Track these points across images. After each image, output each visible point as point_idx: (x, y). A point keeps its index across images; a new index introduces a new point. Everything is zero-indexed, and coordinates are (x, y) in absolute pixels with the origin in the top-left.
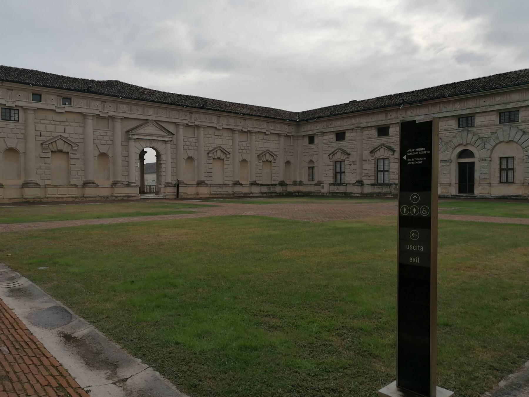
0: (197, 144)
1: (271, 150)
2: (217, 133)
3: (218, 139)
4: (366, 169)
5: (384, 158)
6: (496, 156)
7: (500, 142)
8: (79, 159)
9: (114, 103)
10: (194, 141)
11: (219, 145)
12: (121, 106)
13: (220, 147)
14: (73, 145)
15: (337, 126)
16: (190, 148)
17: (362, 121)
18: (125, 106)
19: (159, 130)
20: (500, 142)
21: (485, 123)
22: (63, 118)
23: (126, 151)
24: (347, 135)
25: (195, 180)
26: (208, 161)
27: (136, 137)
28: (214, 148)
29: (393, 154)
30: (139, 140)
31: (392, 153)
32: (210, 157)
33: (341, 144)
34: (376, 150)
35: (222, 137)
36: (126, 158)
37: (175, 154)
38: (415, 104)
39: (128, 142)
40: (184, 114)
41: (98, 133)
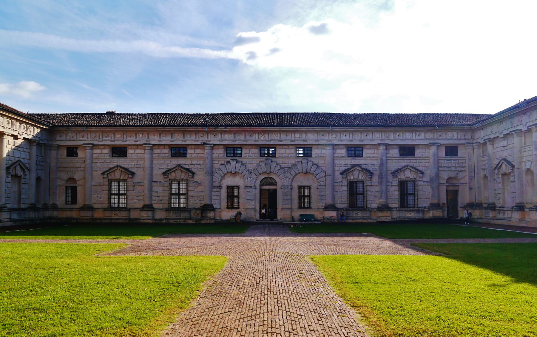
1: (22, 160)
4: (157, 192)
5: (180, 180)
6: (296, 185)
7: (300, 173)
15: (117, 139)
17: (152, 137)
20: (300, 173)
21: (286, 155)
24: (130, 152)
29: (193, 177)
31: (191, 175)
33: (121, 161)
34: (171, 171)
38: (219, 129)
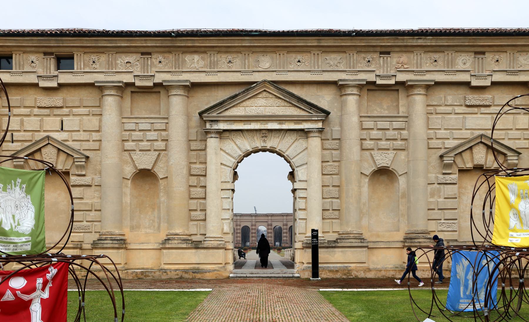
0: (404, 132)
2: (474, 98)
3: (479, 116)
8: (90, 186)
9: (170, 52)
10: (396, 125)
11: (481, 132)
12: (188, 58)
13: (482, 136)
14: (75, 156)
16: (383, 144)
18: (196, 57)
19: (286, 104)
22: (57, 99)
23: (200, 163)
25: (398, 231)
26: (442, 176)
27: (222, 126)
28: (463, 141)
30: (233, 133)
32: (448, 166)
35: (492, 108)
36: (202, 178)
37: (336, 164)
39: (206, 140)
40: (364, 58)
41: (132, 126)
